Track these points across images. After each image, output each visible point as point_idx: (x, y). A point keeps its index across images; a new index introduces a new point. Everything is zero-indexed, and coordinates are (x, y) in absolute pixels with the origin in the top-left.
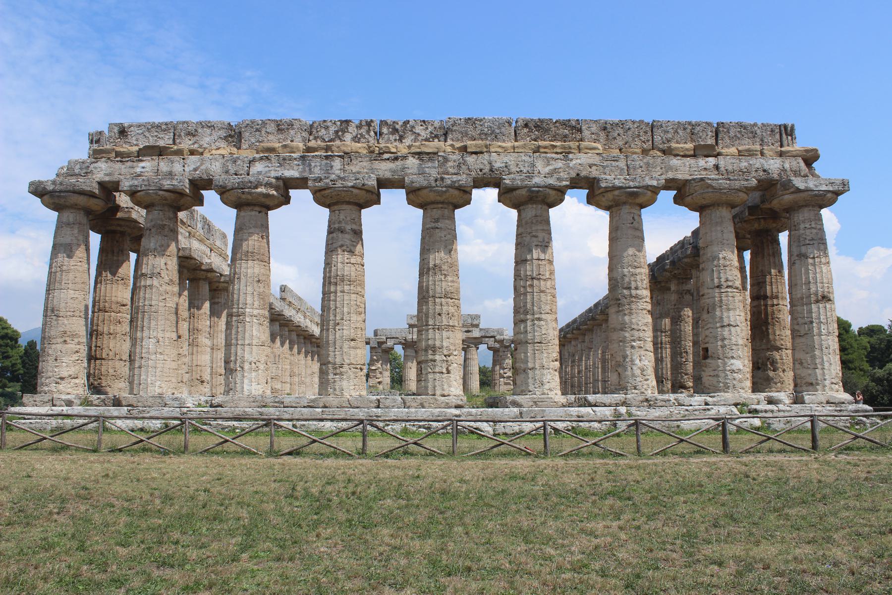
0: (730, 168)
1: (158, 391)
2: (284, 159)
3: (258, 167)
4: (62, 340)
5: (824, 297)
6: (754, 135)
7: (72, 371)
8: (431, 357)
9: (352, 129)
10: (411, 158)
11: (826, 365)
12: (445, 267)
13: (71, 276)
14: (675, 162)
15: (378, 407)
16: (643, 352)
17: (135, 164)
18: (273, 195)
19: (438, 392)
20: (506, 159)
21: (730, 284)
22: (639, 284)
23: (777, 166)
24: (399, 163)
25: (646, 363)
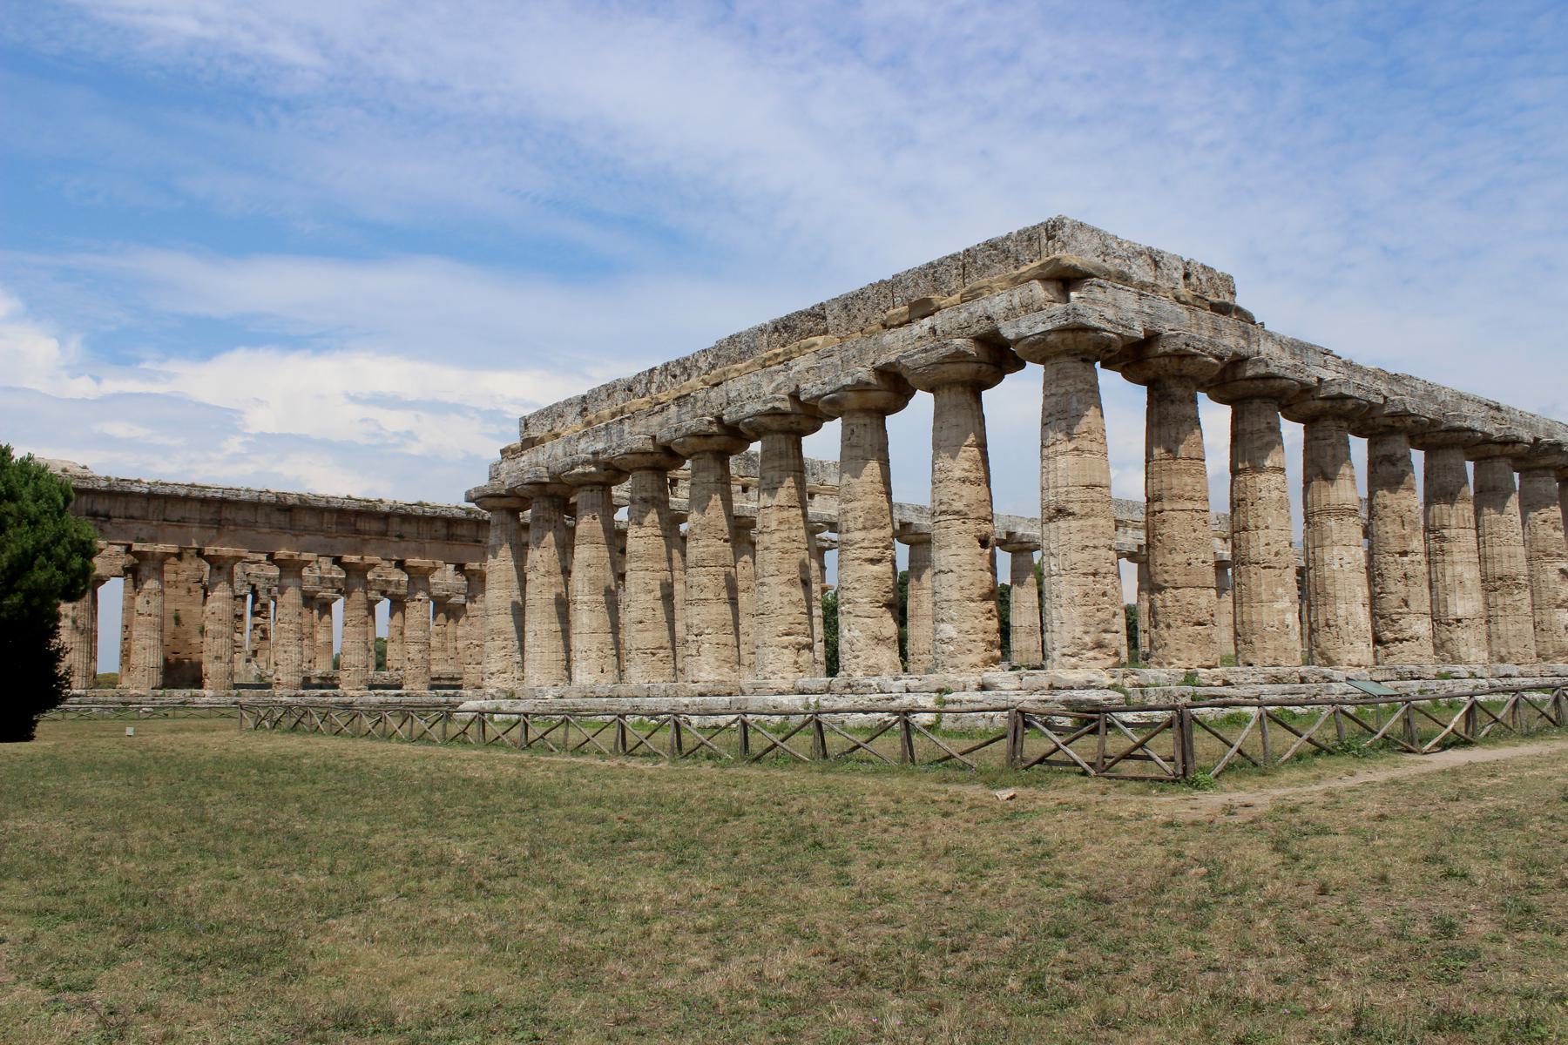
0: (947, 328)
1: (537, 683)
3: (582, 444)
5: (1059, 511)
6: (1006, 252)
7: (500, 666)
9: (656, 378)
11: (1056, 624)
12: (697, 531)
13: (496, 576)
14: (888, 337)
16: (852, 620)
18: (591, 473)
21: (943, 508)
22: (851, 525)
23: (1004, 304)
25: (857, 633)
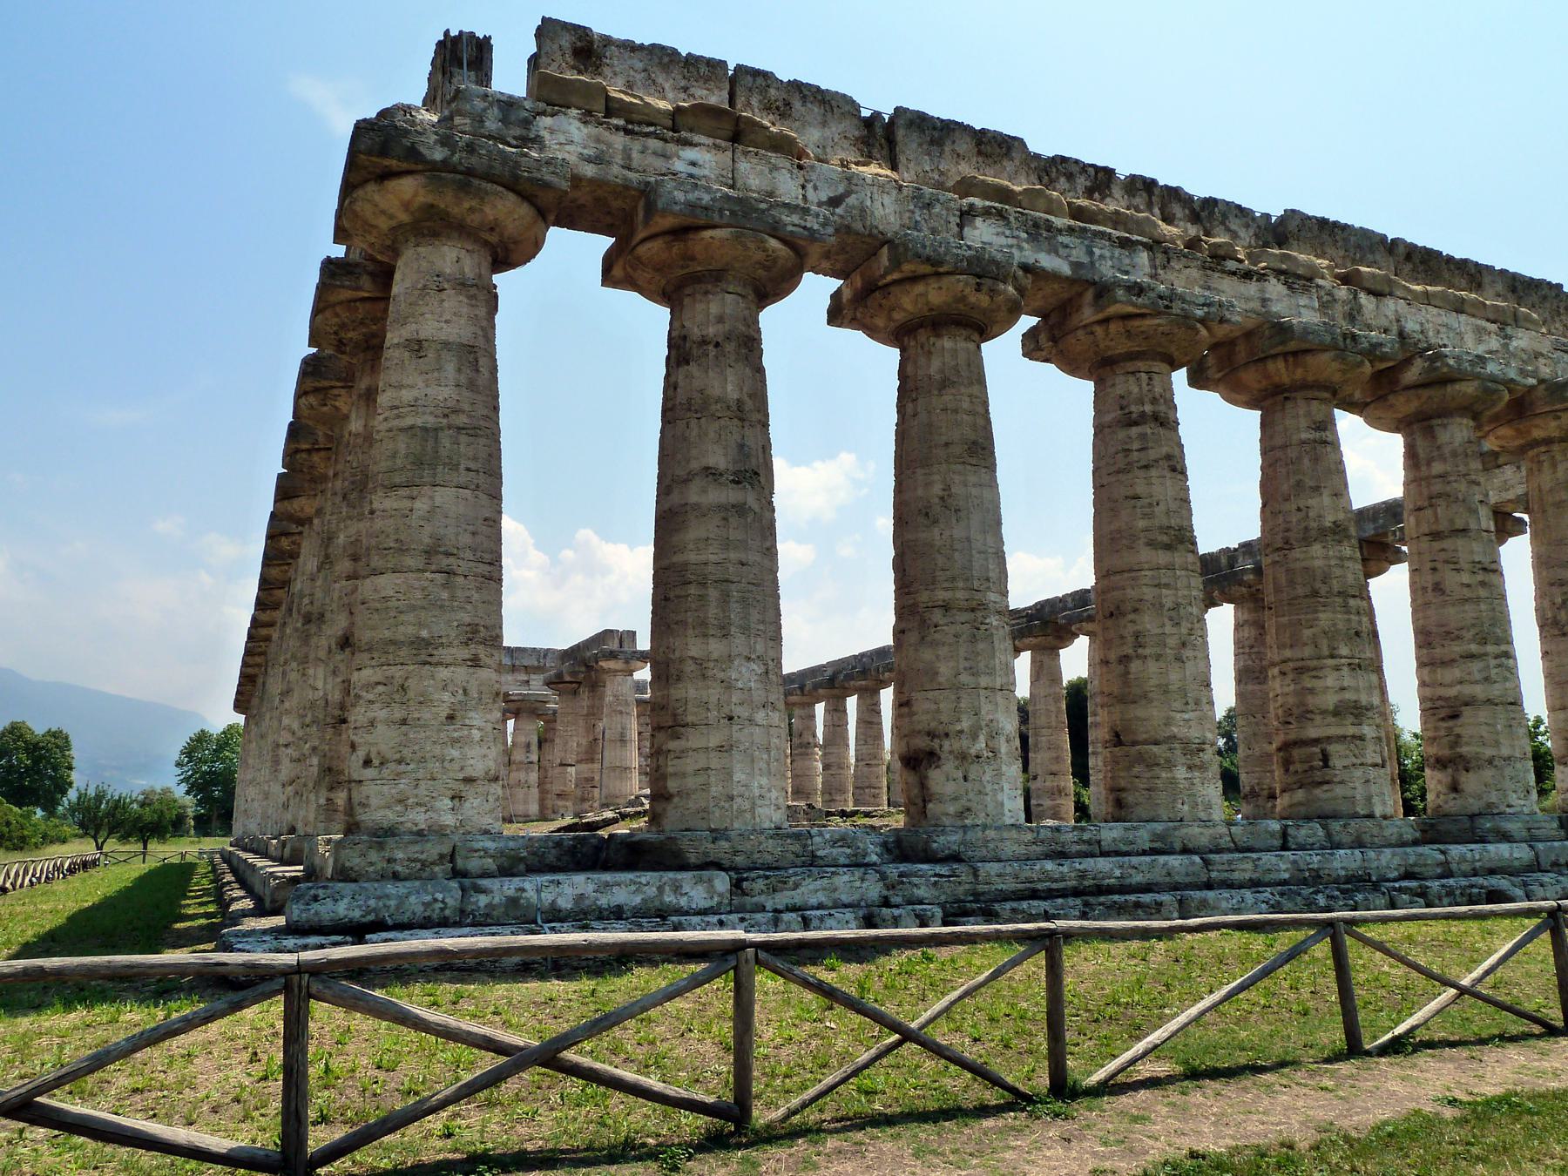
2: (1036, 225)
4: (465, 653)
8: (1351, 730)
10: (1273, 281)
15: (1284, 848)
17: (671, 147)
19: (1378, 811)
20: (1420, 318)
24: (1252, 288)
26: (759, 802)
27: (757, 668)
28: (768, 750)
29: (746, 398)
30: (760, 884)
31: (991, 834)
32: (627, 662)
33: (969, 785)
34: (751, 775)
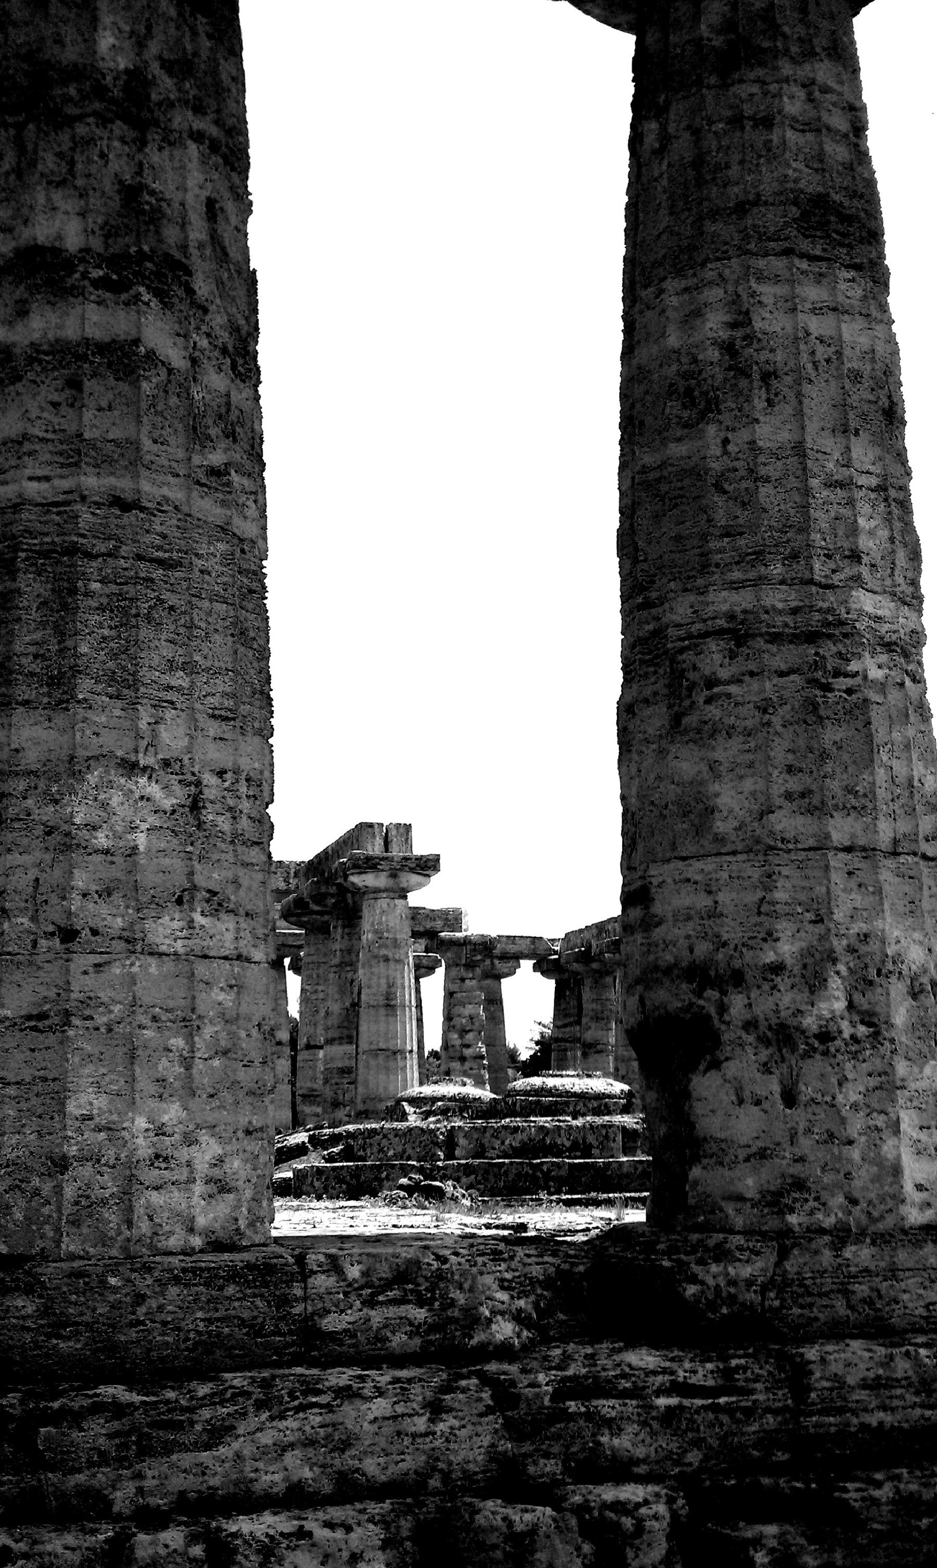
26: (151, 1176)
27: (163, 794)
28: (189, 1024)
29: (155, 68)
30: (96, 1432)
31: (861, 1255)
32: (394, 876)
33: (799, 1117)
34: (128, 1098)
